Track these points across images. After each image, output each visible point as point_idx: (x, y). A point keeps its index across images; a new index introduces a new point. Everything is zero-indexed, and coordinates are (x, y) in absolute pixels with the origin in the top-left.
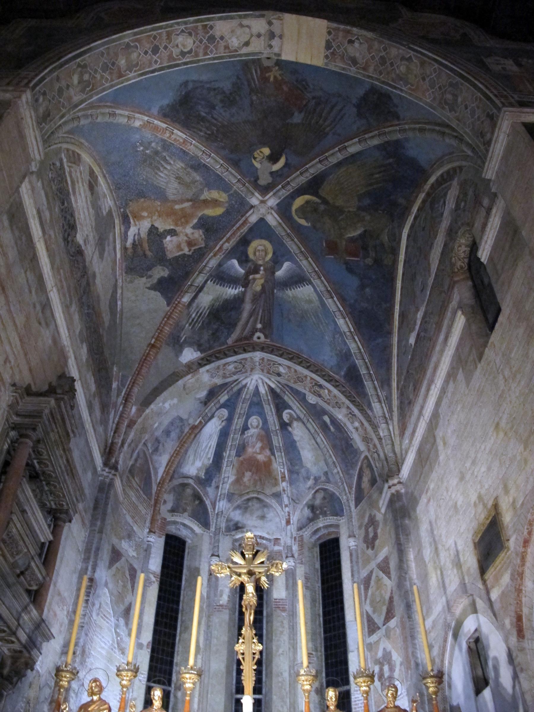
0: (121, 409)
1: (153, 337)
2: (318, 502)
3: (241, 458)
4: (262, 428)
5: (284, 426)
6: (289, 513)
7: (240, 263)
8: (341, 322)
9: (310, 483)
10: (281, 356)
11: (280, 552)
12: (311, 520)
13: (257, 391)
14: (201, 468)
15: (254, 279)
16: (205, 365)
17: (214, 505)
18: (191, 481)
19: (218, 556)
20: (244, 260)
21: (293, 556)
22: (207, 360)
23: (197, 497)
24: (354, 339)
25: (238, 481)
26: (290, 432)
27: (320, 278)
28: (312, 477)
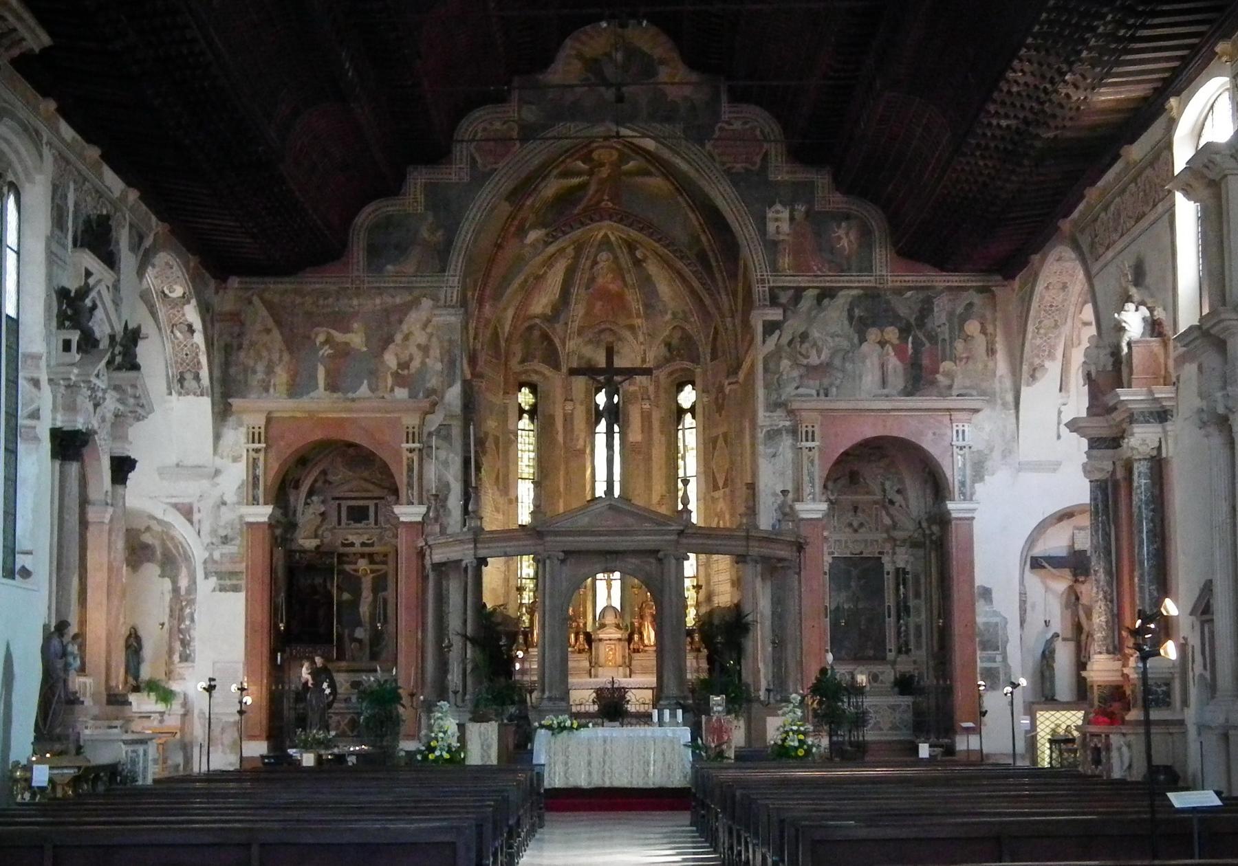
0: (476, 313)
1: (499, 236)
2: (675, 342)
3: (591, 290)
4: (613, 262)
5: (638, 263)
6: (645, 351)
7: (584, 163)
8: (691, 215)
9: (668, 317)
10: (630, 225)
11: (635, 392)
12: (668, 360)
13: (606, 236)
14: (547, 305)
15: (599, 171)
16: (552, 242)
17: (564, 344)
18: (537, 321)
19: (572, 400)
20: (587, 158)
21: (649, 399)
22: (553, 236)
23: (546, 337)
24: (704, 231)
25: (588, 313)
26: (644, 268)
27: (668, 179)
28: (670, 312)
